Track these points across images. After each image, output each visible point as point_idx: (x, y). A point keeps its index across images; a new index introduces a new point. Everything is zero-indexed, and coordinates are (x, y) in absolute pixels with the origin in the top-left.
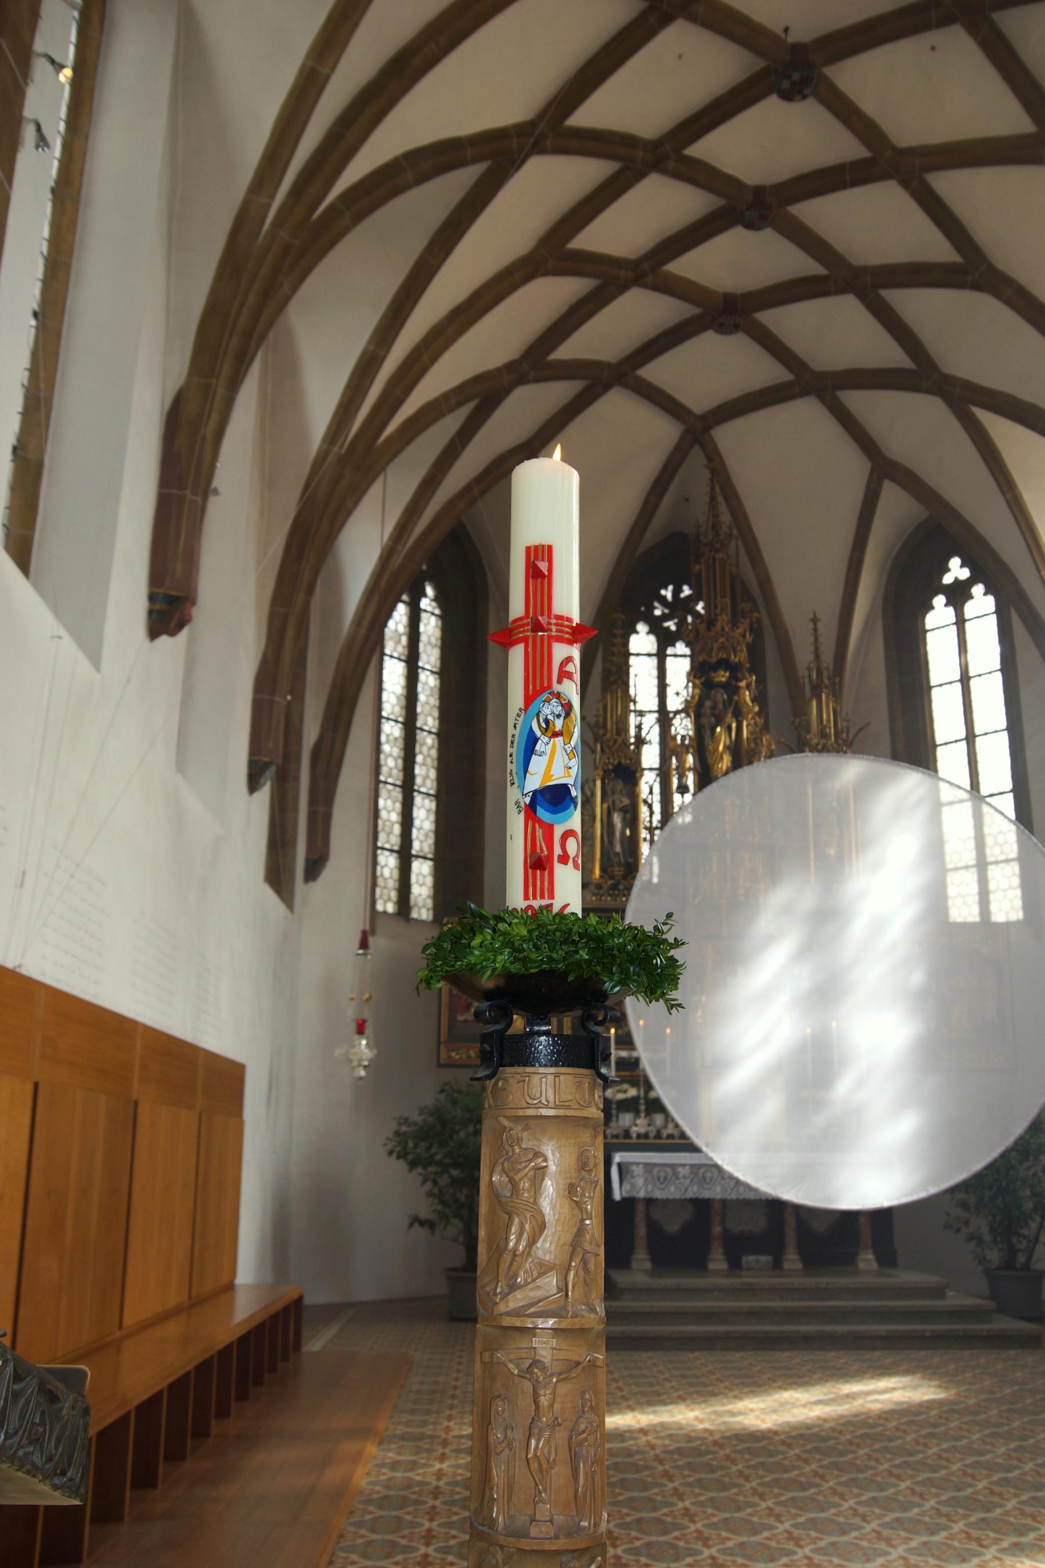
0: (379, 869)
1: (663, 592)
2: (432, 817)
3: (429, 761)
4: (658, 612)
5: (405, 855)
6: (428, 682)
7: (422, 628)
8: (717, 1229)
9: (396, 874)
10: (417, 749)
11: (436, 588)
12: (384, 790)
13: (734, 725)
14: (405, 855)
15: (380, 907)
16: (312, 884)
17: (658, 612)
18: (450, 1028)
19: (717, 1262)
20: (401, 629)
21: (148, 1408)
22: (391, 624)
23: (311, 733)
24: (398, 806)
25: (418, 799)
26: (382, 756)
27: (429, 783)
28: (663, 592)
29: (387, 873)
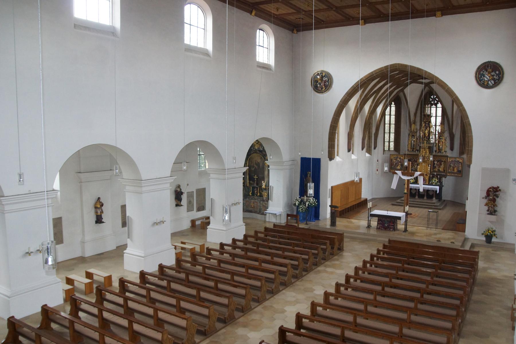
0: (385, 145)
1: (431, 97)
2: (394, 136)
3: (393, 128)
4: (431, 100)
5: (389, 142)
6: (393, 118)
7: (392, 109)
8: (417, 194)
9: (388, 145)
10: (391, 127)
11: (394, 102)
12: (385, 134)
13: (429, 129)
14: (389, 142)
15: (385, 149)
16: (375, 150)
17: (431, 100)
18: (391, 167)
19: (417, 197)
20: (388, 110)
21: (349, 208)
22: (387, 110)
23: (374, 131)
24: (388, 136)
25: (391, 134)
26: (386, 129)
27: (393, 131)
28: (431, 97)
29: (387, 145)
